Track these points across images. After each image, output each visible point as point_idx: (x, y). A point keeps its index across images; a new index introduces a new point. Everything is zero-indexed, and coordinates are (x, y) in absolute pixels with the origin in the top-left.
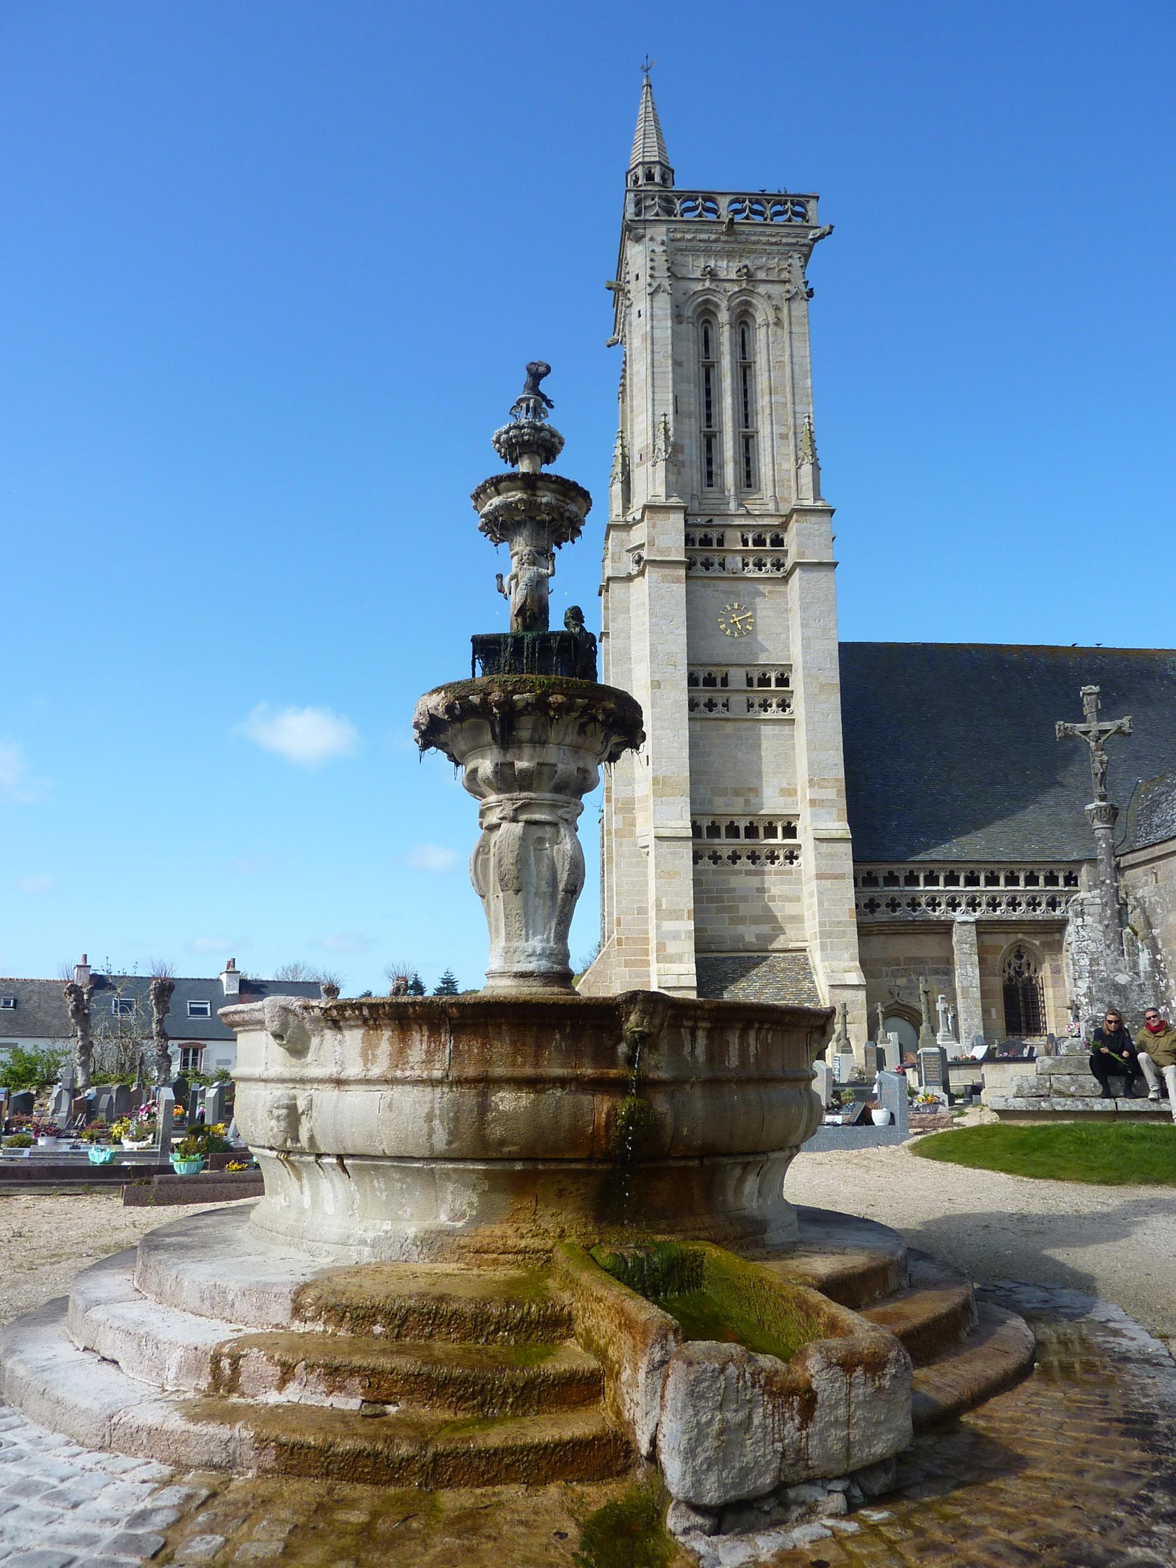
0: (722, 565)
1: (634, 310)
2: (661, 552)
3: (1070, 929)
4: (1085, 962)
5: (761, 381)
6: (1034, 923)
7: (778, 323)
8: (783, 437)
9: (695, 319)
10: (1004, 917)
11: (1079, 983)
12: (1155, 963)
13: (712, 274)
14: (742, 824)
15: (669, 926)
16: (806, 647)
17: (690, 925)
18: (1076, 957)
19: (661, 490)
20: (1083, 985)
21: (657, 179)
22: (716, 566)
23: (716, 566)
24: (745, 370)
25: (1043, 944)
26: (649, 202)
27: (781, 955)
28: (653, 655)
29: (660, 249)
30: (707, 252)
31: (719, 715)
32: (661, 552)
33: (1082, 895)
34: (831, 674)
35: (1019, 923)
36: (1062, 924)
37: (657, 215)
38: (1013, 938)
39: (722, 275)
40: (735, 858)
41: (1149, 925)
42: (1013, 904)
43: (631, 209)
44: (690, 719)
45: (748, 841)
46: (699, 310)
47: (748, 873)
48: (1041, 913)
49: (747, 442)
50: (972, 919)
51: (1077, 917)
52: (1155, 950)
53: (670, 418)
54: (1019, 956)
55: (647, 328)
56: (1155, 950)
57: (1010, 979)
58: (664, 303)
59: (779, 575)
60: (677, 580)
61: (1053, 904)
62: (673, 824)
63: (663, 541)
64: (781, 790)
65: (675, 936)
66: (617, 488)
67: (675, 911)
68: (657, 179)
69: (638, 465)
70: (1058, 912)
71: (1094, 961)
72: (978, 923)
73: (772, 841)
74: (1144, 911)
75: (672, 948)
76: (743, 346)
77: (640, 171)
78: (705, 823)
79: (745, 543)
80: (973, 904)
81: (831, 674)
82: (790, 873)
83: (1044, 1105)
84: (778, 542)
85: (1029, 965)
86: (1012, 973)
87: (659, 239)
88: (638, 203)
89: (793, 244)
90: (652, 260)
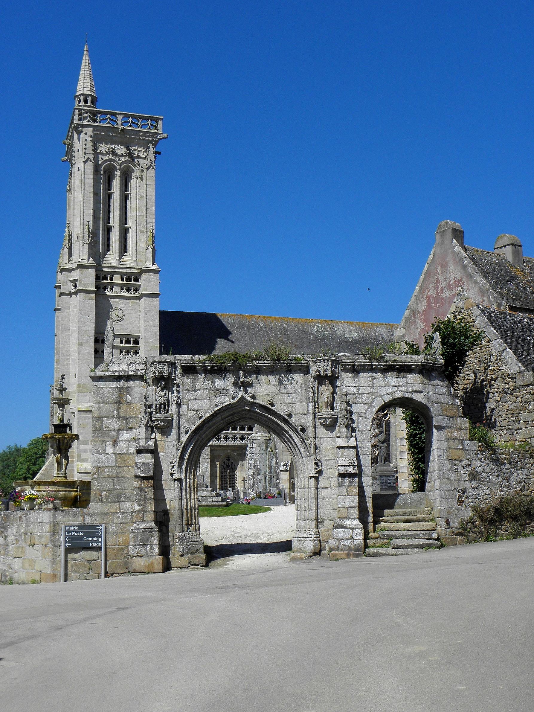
1: (76, 166)
2: (85, 285)
3: (248, 449)
5: (131, 204)
6: (234, 446)
7: (142, 178)
8: (141, 231)
9: (104, 175)
11: (250, 470)
12: (276, 463)
13: (114, 153)
16: (146, 330)
19: (86, 257)
20: (251, 471)
21: (89, 103)
24: (125, 198)
25: (238, 455)
26: (85, 115)
28: (80, 331)
29: (89, 139)
32: (85, 285)
34: (156, 342)
35: (228, 446)
36: (246, 447)
39: (118, 152)
41: (276, 449)
43: (76, 117)
44: (95, 358)
49: (124, 231)
52: (277, 458)
53: (91, 222)
54: (229, 460)
55: (82, 177)
56: (277, 458)
58: (90, 166)
59: (136, 295)
61: (242, 439)
63: (86, 281)
66: (66, 250)
67: (85, 441)
68: (89, 103)
69: (76, 241)
70: (244, 442)
71: (255, 462)
74: (275, 443)
76: (125, 186)
77: (82, 98)
79: (122, 280)
81: (156, 342)
84: (137, 280)
85: (232, 463)
86: (225, 466)
88: (80, 115)
90: (85, 145)
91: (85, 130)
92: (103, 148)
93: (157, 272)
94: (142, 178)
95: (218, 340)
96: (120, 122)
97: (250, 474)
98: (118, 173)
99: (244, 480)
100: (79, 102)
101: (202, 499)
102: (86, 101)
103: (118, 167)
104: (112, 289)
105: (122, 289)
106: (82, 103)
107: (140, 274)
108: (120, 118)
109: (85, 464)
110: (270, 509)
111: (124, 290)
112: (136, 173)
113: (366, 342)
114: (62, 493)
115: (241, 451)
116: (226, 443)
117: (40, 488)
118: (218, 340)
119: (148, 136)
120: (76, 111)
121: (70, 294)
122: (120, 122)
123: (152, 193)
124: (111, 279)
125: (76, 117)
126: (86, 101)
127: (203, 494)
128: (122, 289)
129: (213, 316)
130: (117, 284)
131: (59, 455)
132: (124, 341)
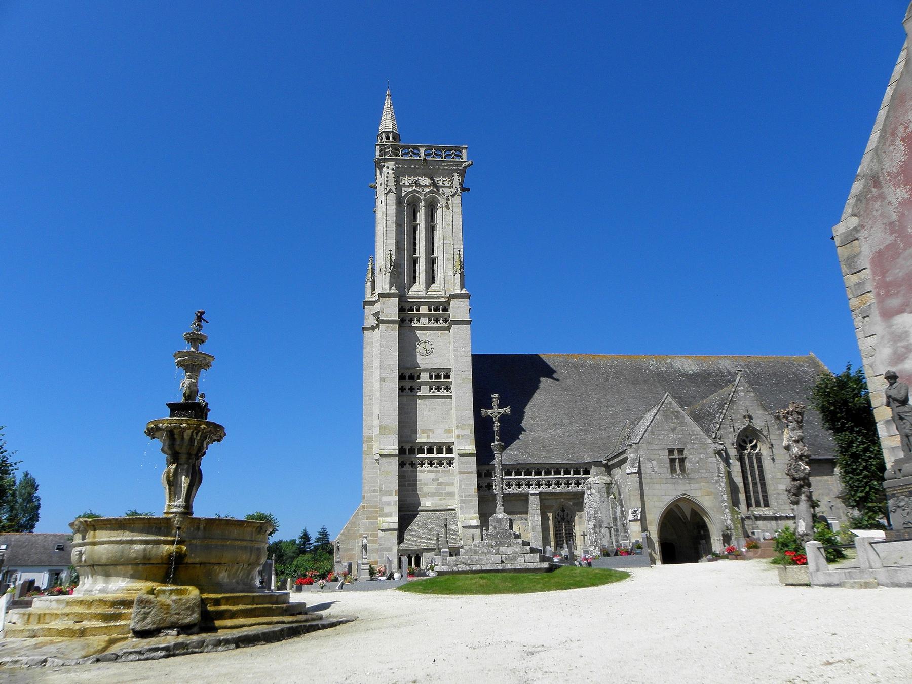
1: (378, 201)
3: (586, 496)
4: (592, 512)
5: (438, 234)
6: (568, 493)
7: (447, 207)
8: (449, 259)
10: (563, 491)
12: (622, 512)
13: (417, 184)
15: (385, 499)
16: (456, 360)
17: (396, 498)
19: (387, 287)
20: (592, 523)
21: (391, 139)
24: (431, 229)
28: (381, 366)
29: (391, 172)
32: (387, 316)
33: (591, 479)
35: (561, 494)
36: (583, 493)
39: (422, 183)
41: (620, 494)
42: (568, 484)
43: (378, 153)
44: (399, 396)
45: (429, 456)
47: (428, 471)
48: (572, 489)
49: (431, 263)
52: (622, 506)
53: (394, 252)
54: (563, 511)
55: (385, 209)
56: (622, 506)
58: (392, 197)
59: (446, 325)
60: (394, 329)
61: (578, 484)
63: (387, 311)
65: (389, 504)
66: (369, 284)
68: (391, 139)
72: (540, 494)
73: (440, 455)
75: (387, 510)
76: (431, 217)
77: (383, 135)
78: (407, 447)
79: (430, 310)
80: (539, 485)
82: (449, 471)
83: (455, 568)
84: (446, 309)
87: (390, 167)
88: (381, 151)
91: (386, 164)
92: (405, 181)
93: (468, 297)
94: (447, 207)
95: (541, 379)
97: (591, 527)
98: (422, 204)
99: (584, 535)
101: (506, 559)
102: (388, 138)
103: (422, 198)
104: (419, 321)
106: (384, 140)
107: (448, 303)
108: (422, 150)
109: (388, 519)
110: (627, 575)
112: (442, 202)
113: (709, 375)
114: (138, 547)
115: (578, 500)
116: (559, 490)
117: (94, 537)
118: (541, 379)
119: (453, 166)
121: (373, 328)
123: (458, 219)
124: (418, 310)
126: (388, 138)
127: (510, 550)
128: (430, 320)
129: (537, 355)
130: (424, 315)
131: (174, 466)
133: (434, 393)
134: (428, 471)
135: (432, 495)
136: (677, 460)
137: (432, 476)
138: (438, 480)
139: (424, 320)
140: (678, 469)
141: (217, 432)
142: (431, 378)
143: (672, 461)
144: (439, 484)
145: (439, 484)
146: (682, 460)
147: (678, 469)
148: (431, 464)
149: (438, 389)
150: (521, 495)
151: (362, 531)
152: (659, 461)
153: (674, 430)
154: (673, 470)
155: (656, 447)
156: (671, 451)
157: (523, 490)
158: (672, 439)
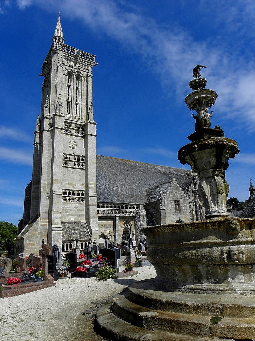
0: (70, 131)
3: (137, 218)
14: (72, 192)
18: (138, 224)
22: (69, 131)
23: (69, 131)
26: (59, 45)
27: (79, 223)
30: (71, 61)
31: (67, 166)
32: (58, 126)
34: (94, 160)
37: (60, 49)
38: (125, 220)
40: (70, 200)
46: (68, 73)
47: (73, 203)
48: (131, 215)
50: (119, 216)
51: (138, 216)
57: (124, 229)
62: (57, 191)
64: (81, 185)
65: (57, 218)
68: (61, 41)
72: (120, 216)
81: (94, 160)
88: (56, 45)
89: (90, 65)
93: (96, 124)
96: (76, 53)
100: (56, 40)
102: (59, 40)
105: (76, 132)
106: (57, 40)
108: (76, 51)
111: (77, 133)
120: (55, 43)
122: (76, 53)
124: (70, 126)
125: (55, 46)
126: (59, 40)
128: (76, 132)
132: (76, 159)
133: (76, 166)
134: (73, 203)
135: (74, 215)
136: (177, 206)
137: (74, 206)
138: (77, 208)
139: (73, 131)
140: (177, 209)
141: (238, 154)
142: (75, 159)
143: (176, 205)
144: (78, 210)
145: (78, 210)
146: (179, 205)
147: (177, 209)
148: (74, 200)
149: (78, 165)
150: (112, 216)
151: (39, 231)
152: (172, 205)
153: (176, 193)
154: (176, 209)
155: (171, 199)
156: (175, 201)
157: (113, 214)
158: (175, 197)
